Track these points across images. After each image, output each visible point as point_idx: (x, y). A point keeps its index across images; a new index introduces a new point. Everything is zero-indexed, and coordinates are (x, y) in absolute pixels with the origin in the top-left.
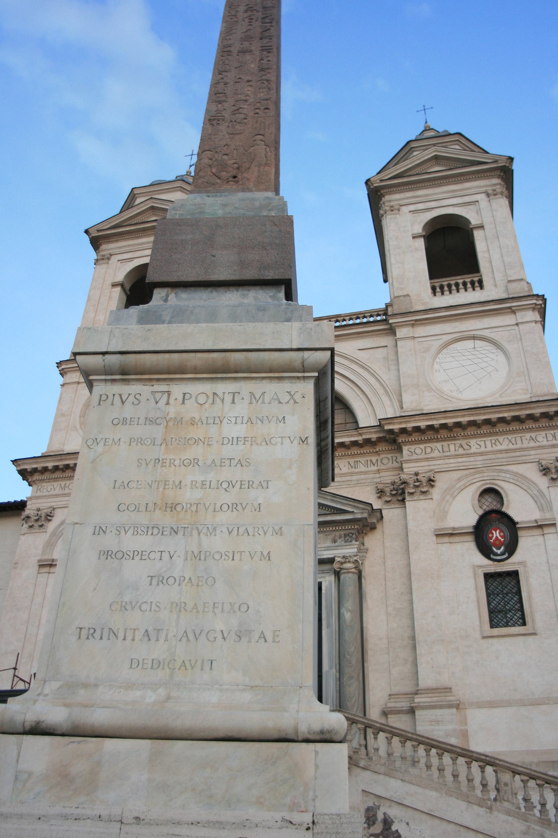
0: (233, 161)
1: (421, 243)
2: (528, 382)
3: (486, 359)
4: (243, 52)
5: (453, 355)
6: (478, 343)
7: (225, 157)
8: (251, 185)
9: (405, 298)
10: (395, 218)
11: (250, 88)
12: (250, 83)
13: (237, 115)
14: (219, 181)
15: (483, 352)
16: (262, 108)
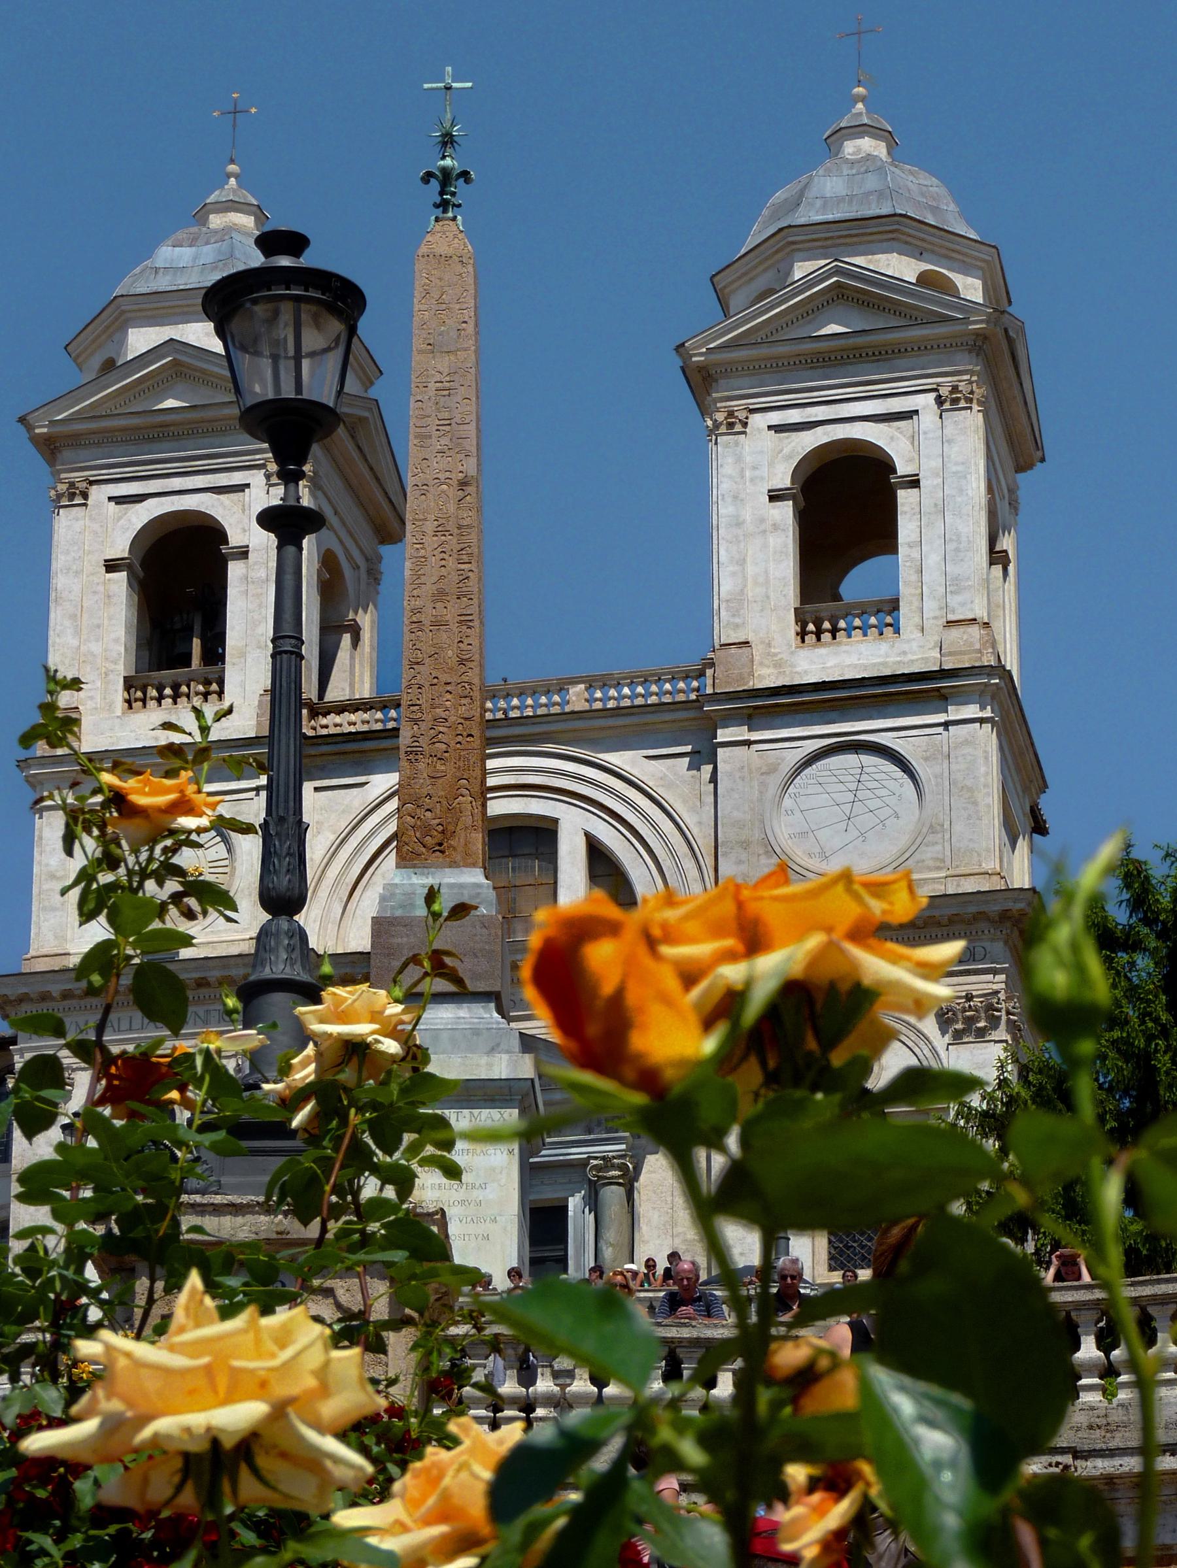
0: (437, 821)
1: (785, 512)
2: (947, 845)
3: (883, 792)
4: (438, 624)
5: (821, 780)
6: (868, 760)
7: (428, 814)
8: (458, 858)
9: (740, 651)
10: (737, 444)
11: (448, 696)
12: (449, 688)
13: (437, 745)
14: (424, 850)
15: (877, 776)
16: (465, 734)
